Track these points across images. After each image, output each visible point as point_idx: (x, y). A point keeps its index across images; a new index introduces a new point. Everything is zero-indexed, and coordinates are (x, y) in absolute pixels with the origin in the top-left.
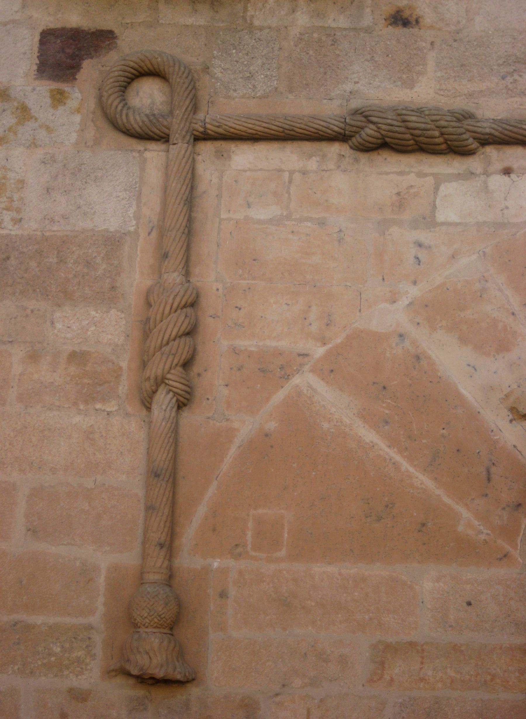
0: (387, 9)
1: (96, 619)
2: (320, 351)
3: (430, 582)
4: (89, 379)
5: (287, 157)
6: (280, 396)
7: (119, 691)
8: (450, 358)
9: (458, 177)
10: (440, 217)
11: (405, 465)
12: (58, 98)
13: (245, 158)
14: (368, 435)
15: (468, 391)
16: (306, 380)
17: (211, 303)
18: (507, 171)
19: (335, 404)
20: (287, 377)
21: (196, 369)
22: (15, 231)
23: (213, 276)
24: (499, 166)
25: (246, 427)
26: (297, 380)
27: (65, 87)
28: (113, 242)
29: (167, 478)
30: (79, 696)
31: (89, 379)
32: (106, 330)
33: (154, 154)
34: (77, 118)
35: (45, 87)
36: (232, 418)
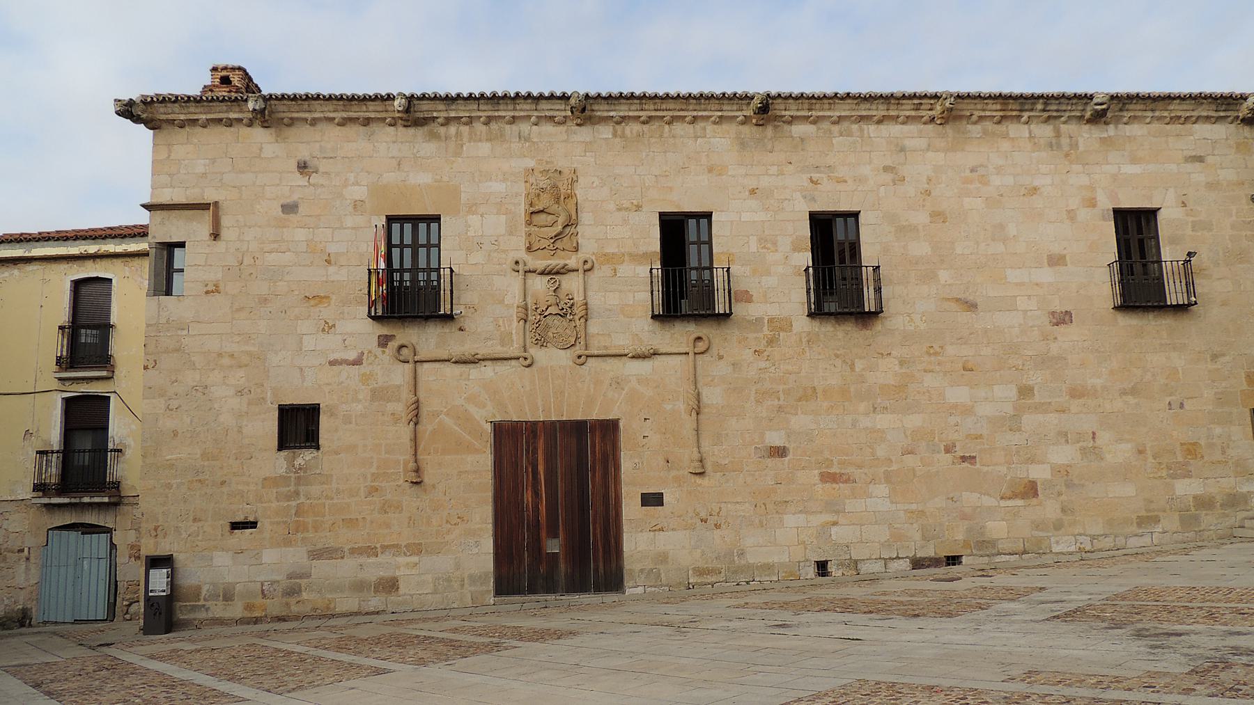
3: (470, 458)
4: (396, 419)
5: (437, 365)
8: (472, 409)
13: (426, 365)
17: (421, 399)
19: (448, 421)
25: (430, 428)
28: (399, 387)
29: (415, 440)
31: (396, 419)
32: (399, 408)
36: (427, 427)
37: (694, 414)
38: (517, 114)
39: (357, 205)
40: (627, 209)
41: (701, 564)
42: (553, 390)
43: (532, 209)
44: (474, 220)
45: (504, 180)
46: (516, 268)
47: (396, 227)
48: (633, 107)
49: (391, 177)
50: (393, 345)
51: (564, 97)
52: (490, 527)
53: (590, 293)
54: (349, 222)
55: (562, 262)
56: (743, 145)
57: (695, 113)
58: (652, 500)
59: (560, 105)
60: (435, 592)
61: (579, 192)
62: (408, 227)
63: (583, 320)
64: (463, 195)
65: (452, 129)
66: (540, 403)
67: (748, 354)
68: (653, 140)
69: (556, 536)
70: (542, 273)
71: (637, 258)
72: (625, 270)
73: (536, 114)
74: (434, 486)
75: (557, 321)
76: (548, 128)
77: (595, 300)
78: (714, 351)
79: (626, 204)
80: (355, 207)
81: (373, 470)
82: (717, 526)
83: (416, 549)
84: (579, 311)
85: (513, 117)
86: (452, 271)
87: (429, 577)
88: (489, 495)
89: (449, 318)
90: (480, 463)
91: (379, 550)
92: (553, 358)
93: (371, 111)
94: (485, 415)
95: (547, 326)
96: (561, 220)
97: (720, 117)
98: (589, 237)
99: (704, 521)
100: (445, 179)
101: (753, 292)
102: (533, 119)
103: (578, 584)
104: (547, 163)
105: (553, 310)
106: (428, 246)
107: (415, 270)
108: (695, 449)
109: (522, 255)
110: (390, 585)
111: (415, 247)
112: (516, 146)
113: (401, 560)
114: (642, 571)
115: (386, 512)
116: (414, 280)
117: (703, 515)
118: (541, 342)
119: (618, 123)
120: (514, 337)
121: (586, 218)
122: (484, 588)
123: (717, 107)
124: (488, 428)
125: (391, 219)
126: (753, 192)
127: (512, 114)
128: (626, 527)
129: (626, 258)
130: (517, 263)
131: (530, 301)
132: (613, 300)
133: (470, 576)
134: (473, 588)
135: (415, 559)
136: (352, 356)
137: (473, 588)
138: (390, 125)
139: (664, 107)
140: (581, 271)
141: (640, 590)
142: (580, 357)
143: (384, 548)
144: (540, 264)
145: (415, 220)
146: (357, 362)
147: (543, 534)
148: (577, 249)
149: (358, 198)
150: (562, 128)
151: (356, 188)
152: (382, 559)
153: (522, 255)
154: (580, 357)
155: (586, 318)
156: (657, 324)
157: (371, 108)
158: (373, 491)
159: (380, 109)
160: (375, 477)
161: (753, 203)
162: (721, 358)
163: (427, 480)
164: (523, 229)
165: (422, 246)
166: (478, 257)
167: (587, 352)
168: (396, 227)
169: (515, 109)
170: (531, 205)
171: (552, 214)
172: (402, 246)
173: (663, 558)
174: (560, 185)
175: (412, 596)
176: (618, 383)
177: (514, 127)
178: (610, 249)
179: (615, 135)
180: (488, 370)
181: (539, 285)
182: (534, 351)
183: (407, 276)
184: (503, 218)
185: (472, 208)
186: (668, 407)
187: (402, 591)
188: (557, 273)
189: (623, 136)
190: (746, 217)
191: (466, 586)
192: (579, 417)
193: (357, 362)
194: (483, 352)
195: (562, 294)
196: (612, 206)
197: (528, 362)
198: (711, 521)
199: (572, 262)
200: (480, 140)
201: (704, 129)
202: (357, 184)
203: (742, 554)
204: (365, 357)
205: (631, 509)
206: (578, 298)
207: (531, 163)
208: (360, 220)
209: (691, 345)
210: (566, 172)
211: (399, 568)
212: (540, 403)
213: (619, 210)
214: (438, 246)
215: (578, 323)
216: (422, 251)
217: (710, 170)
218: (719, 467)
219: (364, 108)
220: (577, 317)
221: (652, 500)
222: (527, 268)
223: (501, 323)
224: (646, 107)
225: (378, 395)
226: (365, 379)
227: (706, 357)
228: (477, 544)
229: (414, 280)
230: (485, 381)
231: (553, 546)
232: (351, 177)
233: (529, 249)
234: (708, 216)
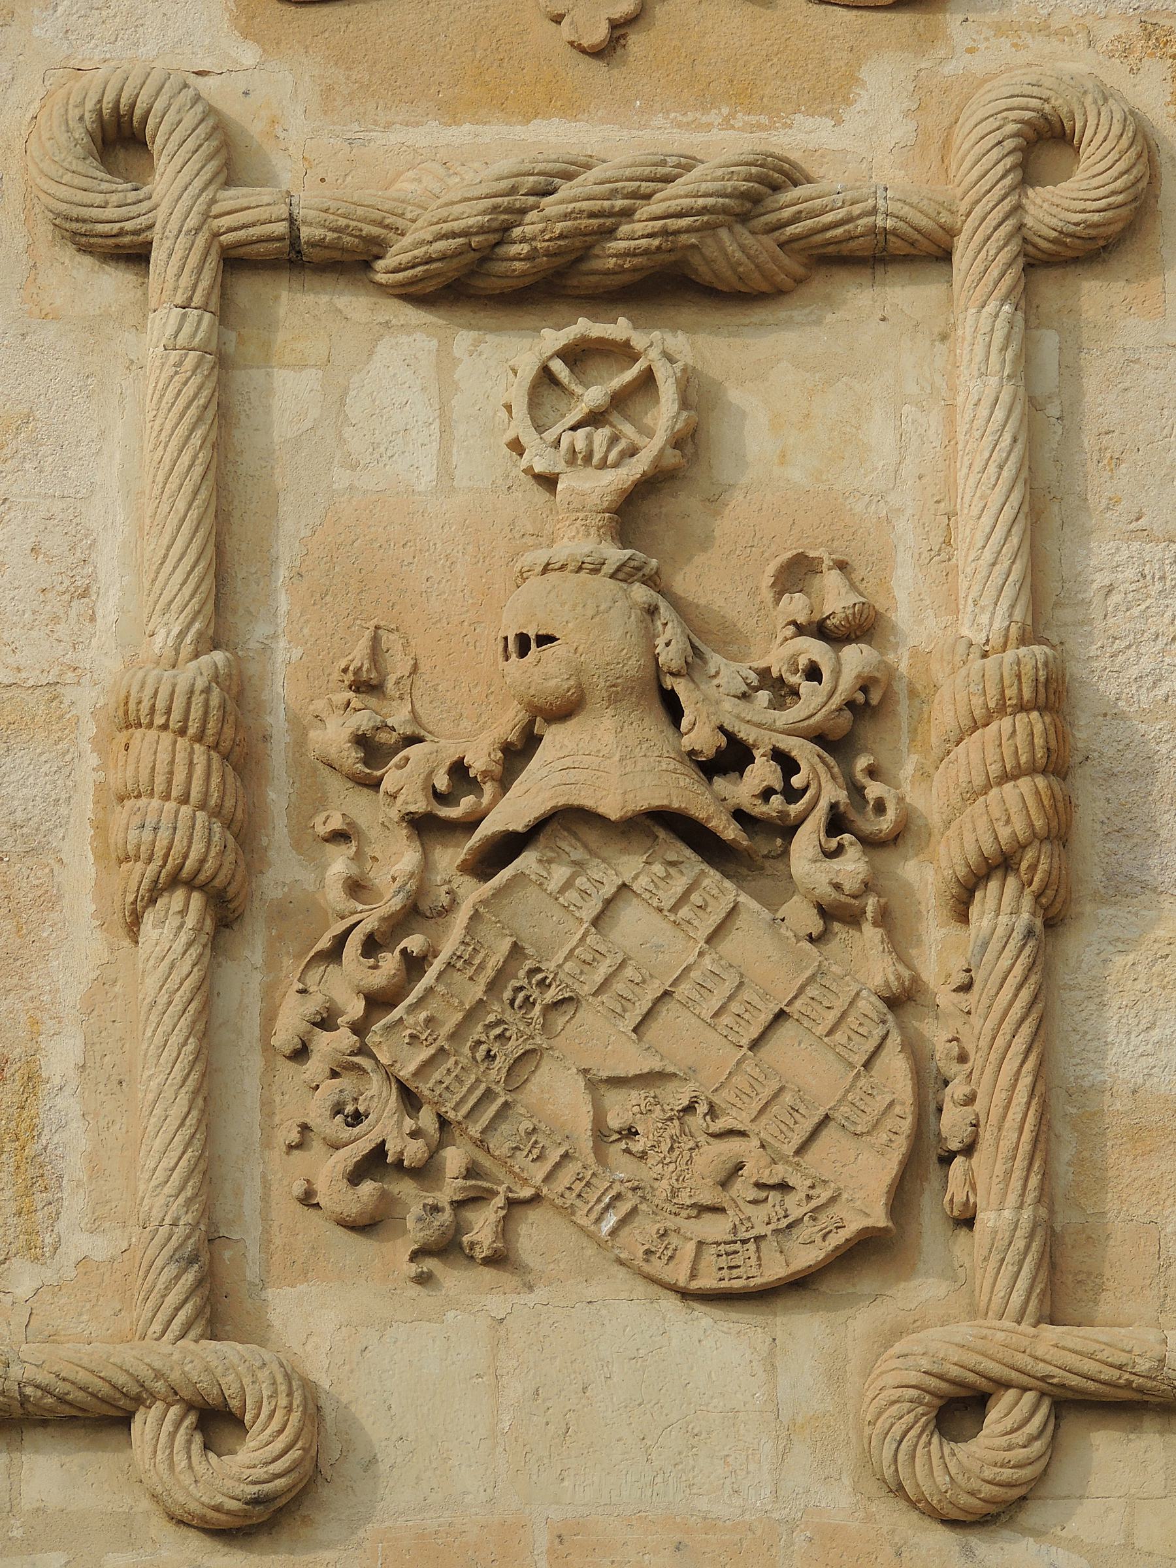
46: (110, 202)
53: (1107, 559)
55: (717, 146)
63: (1002, 911)
70: (471, 280)
75: (660, 913)
84: (951, 785)
95: (526, 991)
105: (606, 762)
118: (436, 1203)
120: (69, 1130)
131: (297, 666)
140: (981, 260)
144: (433, 168)
154: (958, 1407)
155: (1051, 879)
167: (1060, 1350)
182: (338, 1323)
188: (670, 282)
195: (725, 575)
197: (250, 1464)
206: (948, 620)
215: (939, 951)
220: (925, 876)
222: (253, 211)
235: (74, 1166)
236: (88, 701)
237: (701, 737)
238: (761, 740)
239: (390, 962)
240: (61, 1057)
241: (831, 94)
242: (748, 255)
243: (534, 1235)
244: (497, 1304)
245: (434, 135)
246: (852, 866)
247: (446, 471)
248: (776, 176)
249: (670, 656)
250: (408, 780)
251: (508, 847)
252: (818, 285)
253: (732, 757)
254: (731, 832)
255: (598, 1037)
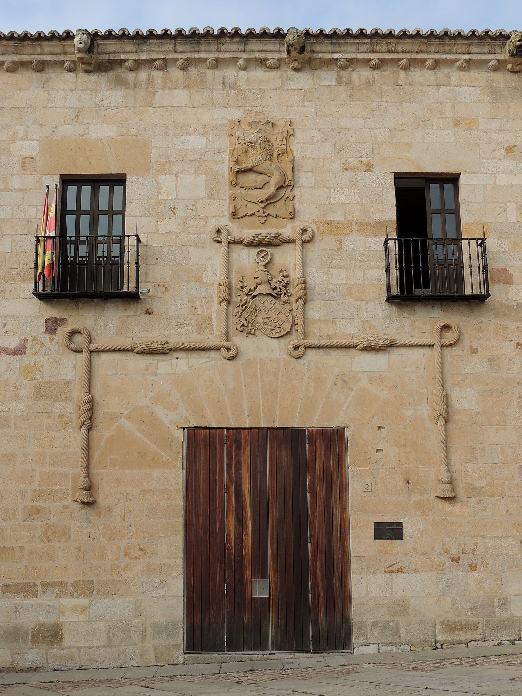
0: (145, 309)
1: (69, 487)
2: (126, 412)
3: (156, 474)
5: (117, 356)
6: (116, 425)
7: (77, 506)
9: (163, 360)
10: (159, 372)
11: (149, 443)
12: (52, 339)
13: (104, 357)
14: (140, 435)
15: (166, 422)
16: (122, 420)
18: (177, 358)
19: (130, 427)
20: (118, 420)
21: (93, 418)
22: (41, 380)
23: (98, 392)
24: (175, 357)
25: (107, 434)
26: (120, 420)
27: (53, 336)
28: (69, 382)
30: (66, 507)
33: (79, 356)
34: (57, 346)
35: (48, 336)
36: (103, 433)
37: (441, 421)
38: (221, 56)
39: (26, 163)
40: (354, 169)
41: (451, 617)
42: (263, 389)
43: (238, 167)
44: (167, 181)
45: (205, 134)
46: (218, 237)
47: (72, 190)
48: (363, 48)
49: (67, 130)
50: (63, 330)
51: (279, 35)
52: (180, 563)
53: (309, 270)
54: (16, 182)
55: (274, 232)
56: (495, 95)
57: (437, 56)
58: (389, 531)
59: (272, 45)
60: (109, 645)
61: (297, 148)
62: (86, 190)
63: (300, 302)
64: (154, 151)
65: (143, 75)
66: (245, 405)
67: (508, 348)
68: (385, 88)
69: (264, 576)
70: (251, 244)
71: (367, 228)
72: (354, 242)
73: (244, 55)
74: (110, 509)
75: (269, 303)
76: (259, 74)
77: (315, 278)
78: (466, 343)
79: (354, 163)
80: (24, 165)
81: (35, 486)
82: (472, 567)
83: (86, 588)
84: (295, 291)
85: (217, 60)
86: (138, 241)
87: (101, 626)
88: (179, 521)
89: (133, 297)
90: (171, 479)
91: (39, 588)
92: (263, 350)
93: (47, 53)
94: (175, 420)
95: (256, 310)
96: (274, 181)
97: (468, 61)
98: (308, 201)
99: (455, 560)
100: (133, 132)
101: (514, 271)
102: (241, 62)
103: (293, 640)
104: (257, 113)
105: (264, 289)
106: (111, 212)
107: (93, 239)
108: (443, 467)
109: (225, 222)
110: (53, 634)
111: (94, 213)
112: (219, 94)
113: (67, 602)
114: (375, 624)
115: (49, 540)
116: (92, 252)
117: (454, 552)
118: (248, 329)
119: (343, 68)
120: (215, 323)
121: (304, 179)
122: (172, 642)
123: (464, 48)
124: (180, 435)
125: (67, 181)
126: (510, 150)
127: (215, 55)
128: (354, 566)
129: (354, 227)
130: (219, 231)
132: (338, 277)
133: (155, 626)
134: (157, 642)
135: (84, 601)
136: (13, 343)
137: (157, 642)
138: (69, 70)
139: (400, 47)
140: (298, 242)
141: (372, 649)
142: (296, 348)
143: (46, 586)
145: (95, 181)
146: (19, 351)
147: (249, 572)
148: (293, 216)
149: (26, 154)
150: (274, 74)
151: (27, 143)
152: (45, 599)
153: (225, 222)
154: (296, 348)
155: (304, 299)
156: (393, 310)
157: (46, 50)
158: (34, 512)
159: (57, 50)
160: (37, 495)
161: (510, 163)
162: (474, 351)
163: (102, 499)
164: (226, 191)
165: (103, 213)
166: (170, 225)
167: (305, 342)
168: (72, 190)
169: (218, 51)
170: (237, 162)
171: (263, 175)
172: (78, 213)
173: (402, 608)
174: (273, 139)
175: (79, 648)
176: (345, 381)
177: (218, 73)
178: (336, 216)
179: (339, 82)
180: (181, 363)
181: (246, 259)
182: (239, 341)
183: (83, 250)
184: (202, 178)
185: (164, 166)
186: (409, 413)
187: (67, 642)
188: (269, 244)
189: (349, 83)
190: (502, 180)
191: (149, 638)
192: (296, 423)
193: (19, 351)
194: (174, 341)
195: (275, 271)
196: (336, 165)
198: (465, 560)
199: (288, 230)
200: (176, 88)
201: (448, 76)
202: (27, 138)
203: (504, 604)
204: (29, 345)
205: (361, 543)
206: (295, 276)
207: (237, 114)
208: (29, 181)
209: (437, 335)
210: (280, 124)
211: (63, 612)
212: (245, 405)
213: (346, 169)
214: (122, 212)
215: (294, 306)
216: (103, 220)
217: (457, 123)
218: (474, 491)
219: (39, 50)
220: (293, 299)
221: (389, 531)
222: (231, 238)
223: (198, 304)
224: (378, 48)
225: (45, 392)
226: (28, 372)
227: (455, 351)
228: (163, 584)
229: (92, 252)
230: (180, 377)
231: (261, 590)
232: (21, 130)
233: (234, 215)
234: (453, 179)
235: (215, 326)
236: (216, 283)
237: (273, 286)
238: (278, 287)
239: (244, 307)
240: (214, 316)
241: (284, 227)
242: (276, 242)
243: (257, 332)
244: (254, 339)
245: (248, 231)
246: (286, 298)
247: (249, 262)
248: (279, 235)
249: (270, 279)
250: (246, 290)
251: (255, 296)
252: (283, 244)
253: (276, 288)
254: (275, 295)
255: (263, 314)
